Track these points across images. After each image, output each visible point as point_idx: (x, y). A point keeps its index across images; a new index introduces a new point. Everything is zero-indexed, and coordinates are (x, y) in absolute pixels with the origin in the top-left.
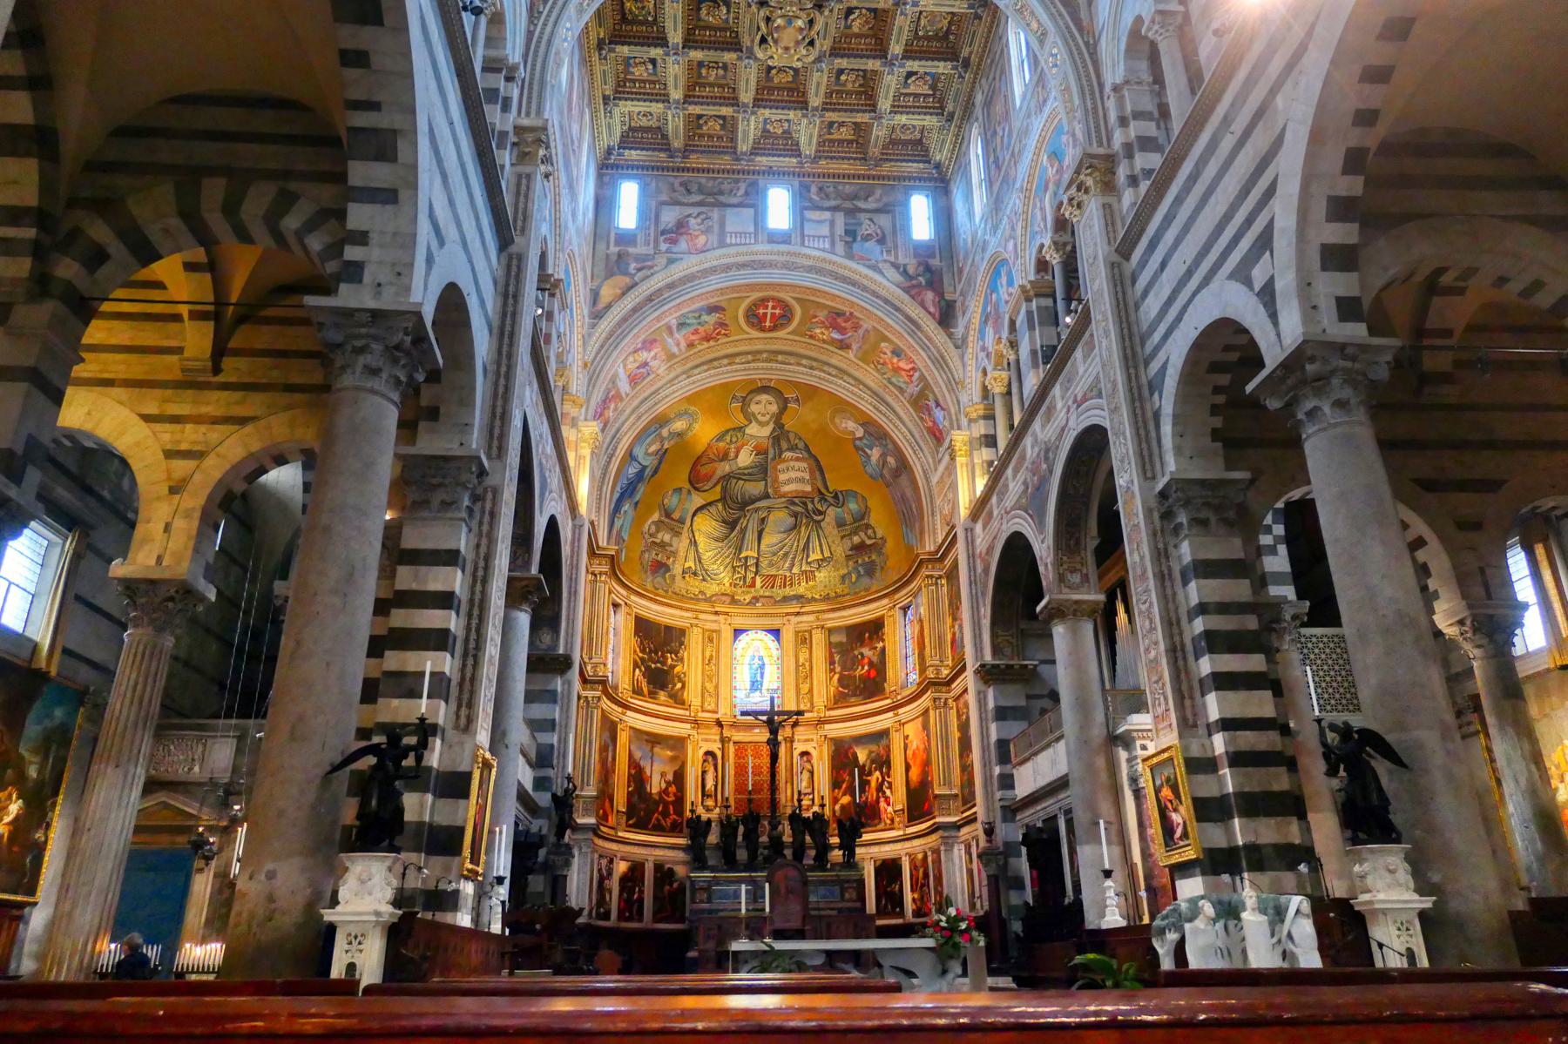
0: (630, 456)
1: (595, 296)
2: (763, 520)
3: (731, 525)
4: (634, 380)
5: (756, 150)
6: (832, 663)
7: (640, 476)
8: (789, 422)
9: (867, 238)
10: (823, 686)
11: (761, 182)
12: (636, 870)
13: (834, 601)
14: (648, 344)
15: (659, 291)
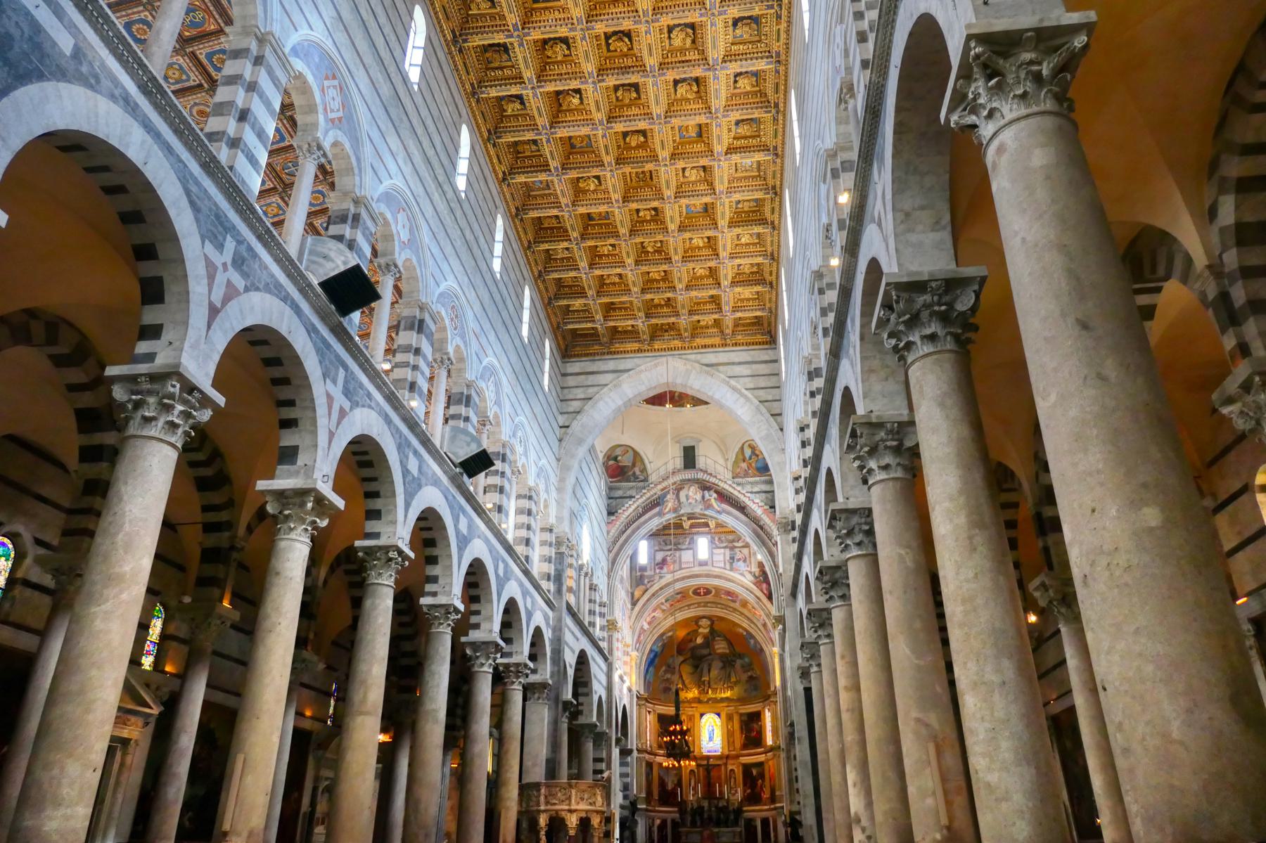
0: (651, 651)
1: (633, 594)
2: (710, 666)
3: (696, 667)
4: (649, 623)
5: (692, 526)
6: (742, 729)
7: (655, 656)
8: (716, 628)
9: (739, 560)
10: (739, 740)
11: (695, 537)
12: (664, 822)
13: (742, 700)
14: (654, 611)
15: (657, 591)
